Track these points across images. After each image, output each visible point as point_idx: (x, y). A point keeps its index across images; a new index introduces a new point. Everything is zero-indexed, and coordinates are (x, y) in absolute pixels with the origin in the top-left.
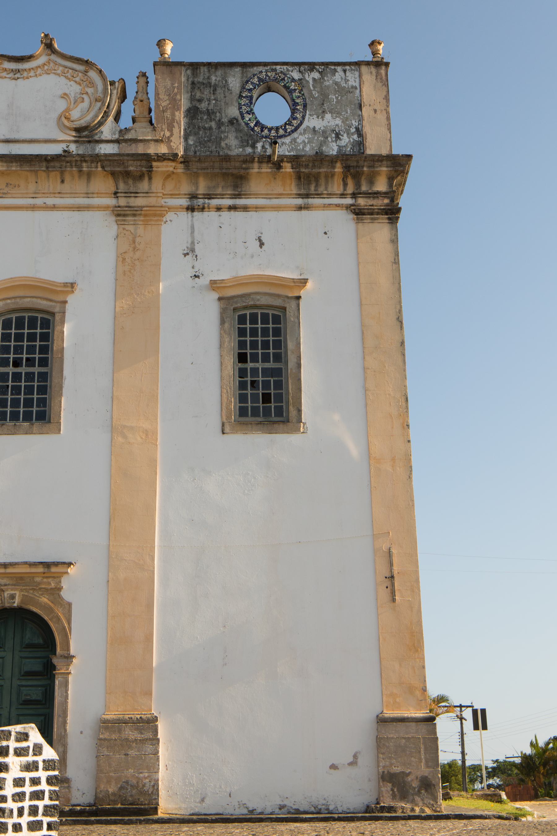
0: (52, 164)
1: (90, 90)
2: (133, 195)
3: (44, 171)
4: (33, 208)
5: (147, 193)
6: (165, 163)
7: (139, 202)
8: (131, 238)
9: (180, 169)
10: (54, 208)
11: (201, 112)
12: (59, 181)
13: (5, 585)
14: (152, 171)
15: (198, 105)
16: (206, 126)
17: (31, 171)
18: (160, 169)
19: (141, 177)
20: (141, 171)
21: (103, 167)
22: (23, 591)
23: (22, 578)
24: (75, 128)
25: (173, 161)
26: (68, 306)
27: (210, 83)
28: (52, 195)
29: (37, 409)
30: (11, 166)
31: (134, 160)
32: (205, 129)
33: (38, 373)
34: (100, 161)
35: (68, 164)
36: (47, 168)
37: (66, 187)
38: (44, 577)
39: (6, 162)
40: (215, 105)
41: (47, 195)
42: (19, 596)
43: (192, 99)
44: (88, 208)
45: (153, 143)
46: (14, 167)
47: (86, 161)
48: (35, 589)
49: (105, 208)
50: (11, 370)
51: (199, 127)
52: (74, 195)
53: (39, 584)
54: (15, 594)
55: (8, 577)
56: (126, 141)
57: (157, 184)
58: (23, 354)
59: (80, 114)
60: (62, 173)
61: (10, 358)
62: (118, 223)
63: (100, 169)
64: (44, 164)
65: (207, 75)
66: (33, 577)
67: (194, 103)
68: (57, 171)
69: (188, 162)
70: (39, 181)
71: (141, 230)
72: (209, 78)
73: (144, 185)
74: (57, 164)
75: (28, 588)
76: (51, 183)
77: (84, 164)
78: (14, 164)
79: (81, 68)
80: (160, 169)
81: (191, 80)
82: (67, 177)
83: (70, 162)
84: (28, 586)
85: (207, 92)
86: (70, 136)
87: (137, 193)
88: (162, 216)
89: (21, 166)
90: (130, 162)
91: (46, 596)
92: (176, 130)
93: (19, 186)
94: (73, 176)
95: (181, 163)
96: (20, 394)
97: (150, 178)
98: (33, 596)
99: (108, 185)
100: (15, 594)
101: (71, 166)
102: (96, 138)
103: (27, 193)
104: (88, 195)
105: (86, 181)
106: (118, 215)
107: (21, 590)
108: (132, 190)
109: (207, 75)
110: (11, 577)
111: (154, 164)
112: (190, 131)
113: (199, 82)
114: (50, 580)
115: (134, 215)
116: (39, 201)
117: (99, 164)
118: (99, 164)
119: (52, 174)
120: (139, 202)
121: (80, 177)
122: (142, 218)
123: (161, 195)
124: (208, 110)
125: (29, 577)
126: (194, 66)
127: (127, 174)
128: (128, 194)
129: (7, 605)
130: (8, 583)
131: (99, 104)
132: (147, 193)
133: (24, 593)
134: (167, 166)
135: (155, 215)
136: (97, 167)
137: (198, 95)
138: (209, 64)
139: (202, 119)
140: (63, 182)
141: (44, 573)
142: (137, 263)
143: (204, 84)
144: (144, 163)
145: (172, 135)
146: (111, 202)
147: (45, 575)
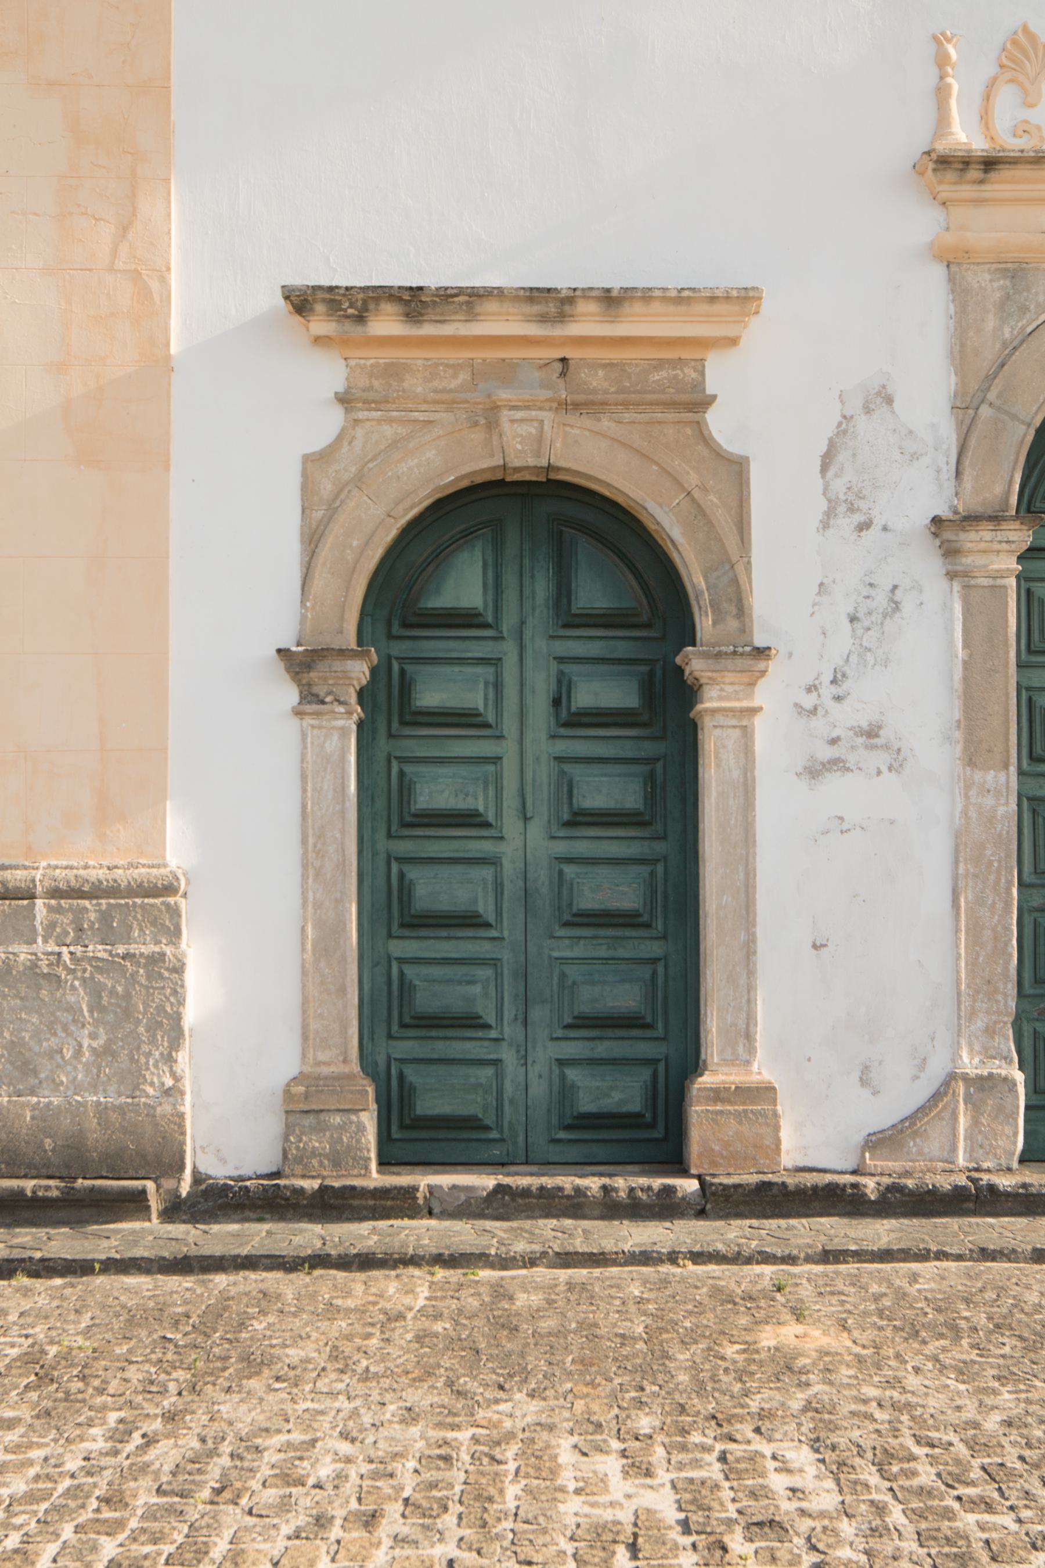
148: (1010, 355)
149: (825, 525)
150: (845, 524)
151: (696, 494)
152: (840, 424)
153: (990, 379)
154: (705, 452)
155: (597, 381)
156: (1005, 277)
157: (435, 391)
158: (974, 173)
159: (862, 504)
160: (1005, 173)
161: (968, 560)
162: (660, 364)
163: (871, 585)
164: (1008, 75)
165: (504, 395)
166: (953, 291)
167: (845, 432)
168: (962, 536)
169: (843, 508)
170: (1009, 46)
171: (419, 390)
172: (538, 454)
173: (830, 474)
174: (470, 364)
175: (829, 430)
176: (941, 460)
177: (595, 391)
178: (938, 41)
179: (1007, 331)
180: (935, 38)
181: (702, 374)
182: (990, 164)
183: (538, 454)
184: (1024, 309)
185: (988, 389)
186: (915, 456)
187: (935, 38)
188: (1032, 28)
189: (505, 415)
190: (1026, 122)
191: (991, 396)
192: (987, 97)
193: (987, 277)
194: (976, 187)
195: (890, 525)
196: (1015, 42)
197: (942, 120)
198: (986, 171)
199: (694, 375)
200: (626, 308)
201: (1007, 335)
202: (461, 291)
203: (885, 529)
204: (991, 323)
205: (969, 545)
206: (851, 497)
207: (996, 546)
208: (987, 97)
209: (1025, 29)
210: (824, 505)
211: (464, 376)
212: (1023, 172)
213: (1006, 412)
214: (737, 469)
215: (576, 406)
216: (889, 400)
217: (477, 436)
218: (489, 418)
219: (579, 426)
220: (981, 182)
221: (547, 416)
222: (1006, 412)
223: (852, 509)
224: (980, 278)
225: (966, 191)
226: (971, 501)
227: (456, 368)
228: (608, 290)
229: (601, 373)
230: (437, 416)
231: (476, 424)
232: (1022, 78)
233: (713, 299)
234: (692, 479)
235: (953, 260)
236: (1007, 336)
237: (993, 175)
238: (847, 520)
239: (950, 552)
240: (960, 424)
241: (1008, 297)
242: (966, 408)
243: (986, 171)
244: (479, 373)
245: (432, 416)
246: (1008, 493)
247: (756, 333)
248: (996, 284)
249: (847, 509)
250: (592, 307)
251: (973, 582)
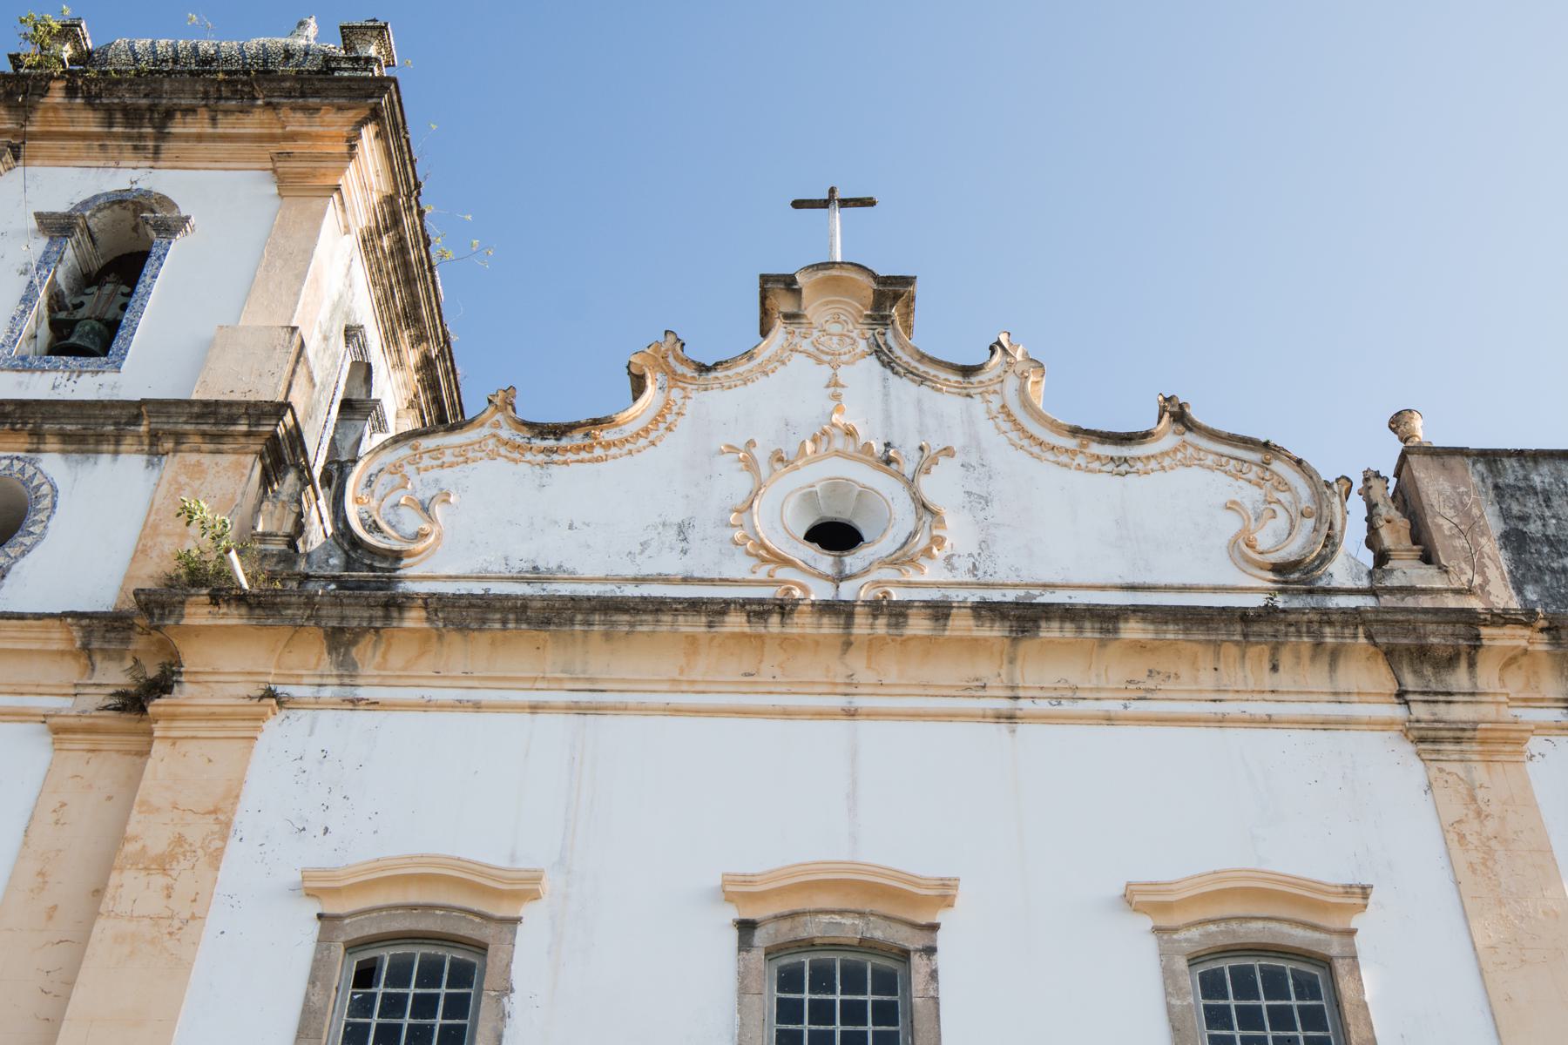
0: (1255, 628)
1: (1284, 497)
2: (1441, 698)
3: (1237, 643)
4: (1221, 721)
5: (1473, 694)
6: (1508, 630)
7: (1459, 712)
8: (1463, 789)
9: (1541, 644)
10: (1269, 721)
11: (1534, 540)
12: (1267, 666)
14: (1481, 646)
15: (1521, 526)
16: (1555, 565)
17: (1209, 641)
18: (1497, 643)
19: (1451, 662)
20: (1456, 648)
21: (1369, 636)
24: (1274, 564)
25: (1526, 625)
26: (1357, 939)
27: (1534, 489)
28: (1257, 696)
30: (1165, 632)
31: (1438, 623)
32: (1553, 571)
34: (1363, 623)
35: (1292, 629)
36: (1245, 635)
37: (1284, 680)
39: (1153, 622)
40: (1558, 526)
41: (1245, 696)
43: (1505, 515)
44: (1346, 723)
45: (1450, 595)
46: (1172, 633)
47: (1330, 623)
49: (1387, 725)
51: (1539, 568)
52: (1306, 695)
56: (1391, 591)
57: (1488, 675)
59: (1283, 538)
60: (1275, 649)
62: (1425, 756)
63: (1362, 640)
64: (1238, 628)
65: (1521, 473)
67: (1513, 523)
68: (1266, 643)
69: (1557, 629)
70: (1221, 666)
71: (1480, 773)
72: (1526, 478)
73: (1459, 679)
74: (1268, 629)
76: (1245, 670)
77: (1327, 630)
78: (1171, 627)
79: (1256, 457)
80: (1497, 643)
81: (1489, 481)
82: (1286, 658)
83: (1296, 624)
85: (1531, 502)
86: (1266, 580)
87: (1450, 694)
88: (1520, 742)
89: (1186, 631)
90: (1431, 627)
92: (1492, 573)
93: (1177, 676)
94: (1298, 658)
95: (1542, 630)
97: (1472, 665)
99: (1379, 678)
101: (1299, 634)
102: (1322, 584)
103: (1200, 691)
104: (1337, 697)
105: (1327, 668)
106: (1422, 740)
108: (1434, 686)
109: (1521, 473)
111: (1484, 631)
112: (1523, 575)
113: (1508, 486)
115: (1458, 740)
116: (1230, 708)
117: (1361, 630)
118: (1361, 630)
119: (1253, 651)
120: (1459, 712)
121: (1313, 658)
122: (1476, 747)
123: (1504, 699)
124: (1547, 537)
126: (1490, 458)
127: (1421, 654)
128: (1431, 696)
131: (1310, 523)
132: (1473, 694)
134: (1513, 637)
135: (1506, 741)
136: (1355, 636)
137: (1515, 508)
138: (1520, 454)
139: (1539, 552)
140: (1275, 668)
142: (1493, 843)
143: (1520, 489)
144: (1461, 629)
145: (1486, 581)
146: (1399, 712)
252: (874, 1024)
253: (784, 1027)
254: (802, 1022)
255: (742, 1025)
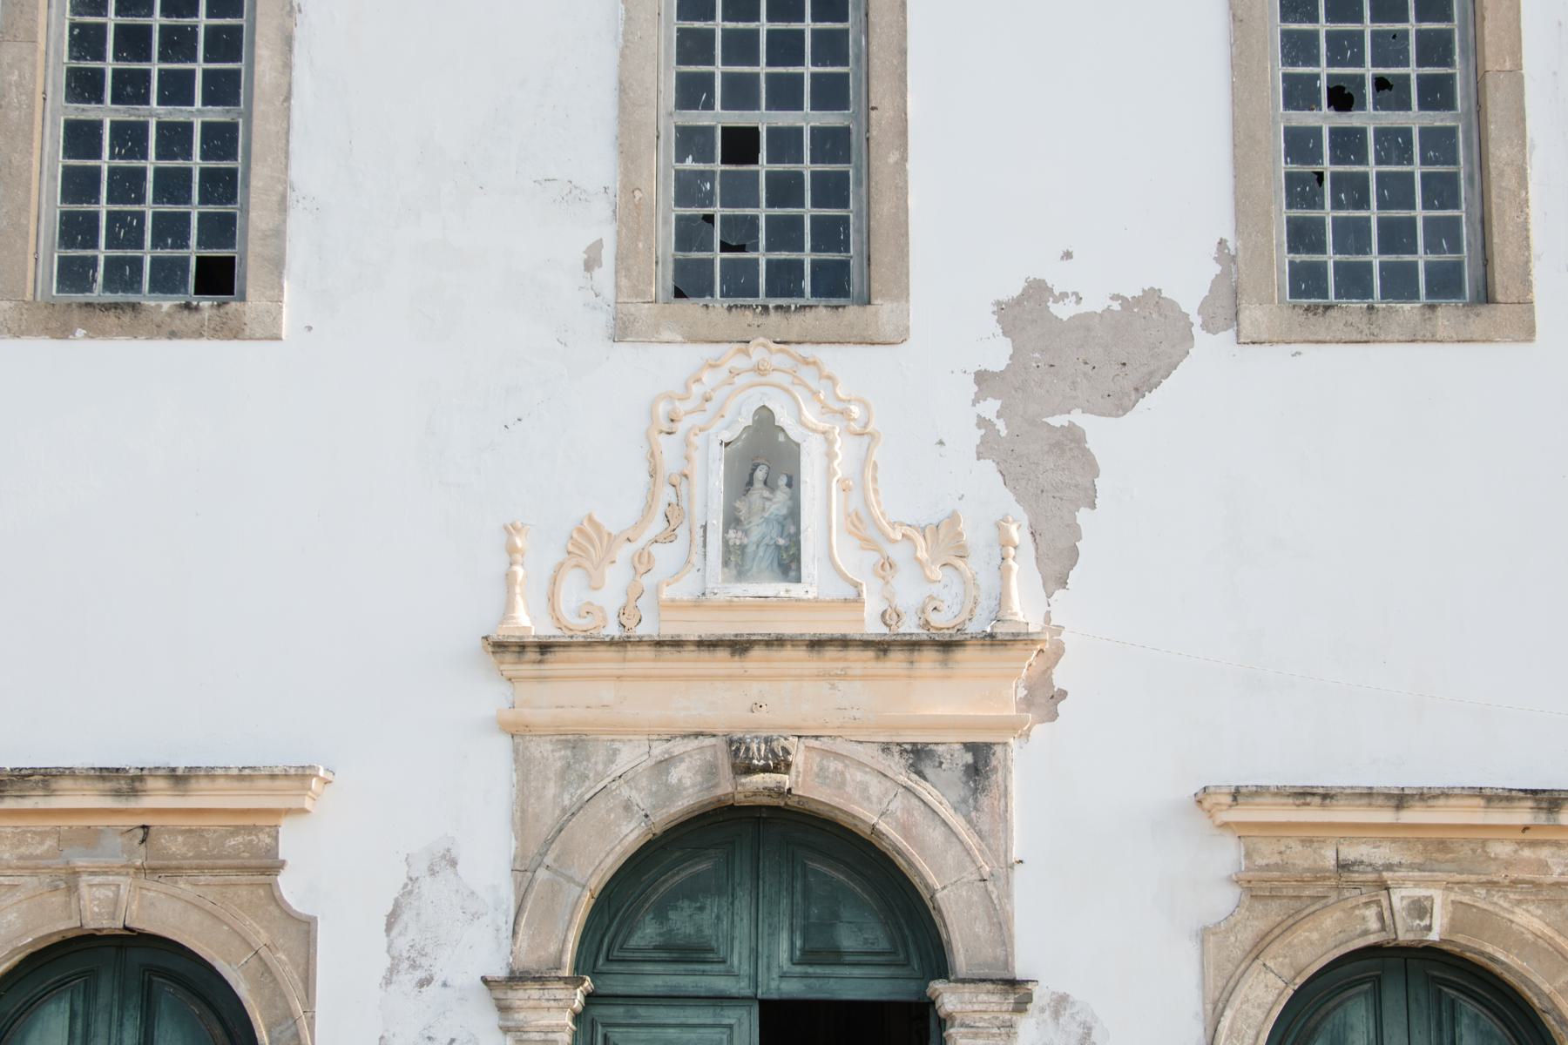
13: (1389, 867)
22: (1451, 889)
23: (1443, 845)
29: (1432, 258)
33: (1423, 131)
38: (1521, 844)
42: (1443, 906)
48: (1494, 883)
50: (1325, 118)
53: (1508, 864)
54: (1431, 899)
55: (1394, 840)
58: (1361, 64)
61: (1317, 77)
66: (1484, 842)
75: (1473, 878)
84: (1471, 872)
91: (1532, 908)
96: (1363, 203)
98: (1491, 908)
100: (1431, 899)
107: (1449, 886)
110: (1406, 840)
114: (1544, 853)
125: (1468, 841)
129: (1405, 937)
130: (1395, 860)
133: (1459, 898)
141: (1526, 828)
147: (1528, 836)
148: (569, 820)
149: (388, 981)
150: (407, 980)
151: (263, 953)
152: (406, 885)
153: (549, 843)
154: (277, 912)
155: (176, 846)
156: (566, 748)
157: (21, 858)
158: (532, 655)
159: (424, 961)
160: (560, 654)
161: (520, 1016)
162: (237, 830)
163: (429, 1038)
164: (574, 561)
165: (80, 862)
166: (516, 761)
167: (410, 893)
168: (511, 994)
169: (406, 965)
170: (575, 535)
171: (6, 856)
172: (113, 917)
173: (394, 933)
174: (57, 831)
175: (395, 892)
176: (501, 920)
177: (173, 856)
178: (511, 530)
179: (566, 797)
180: (506, 528)
181: (276, 839)
182: (545, 647)
183: (113, 917)
184: (584, 778)
185: (545, 853)
186: (476, 916)
187: (506, 528)
188: (596, 518)
189: (84, 880)
190: (591, 604)
191: (548, 860)
192: (554, 582)
193: (549, 747)
194: (536, 666)
195: (449, 982)
196: (581, 531)
197: (509, 606)
198: (542, 653)
199: (268, 840)
200: (193, 784)
201: (567, 802)
202: (35, 771)
203: (445, 985)
204: (551, 790)
205: (518, 1003)
206: (414, 954)
207: (546, 1004)
208: (554, 582)
209: (590, 519)
210: (387, 962)
211: (50, 843)
212: (574, 653)
213: (563, 875)
214: (306, 928)
215: (154, 870)
216: (453, 863)
217: (58, 899)
218: (70, 881)
219: (155, 890)
220: (540, 662)
221: (125, 882)
222: (563, 875)
223: (414, 966)
224: (542, 749)
225: (527, 669)
226: (528, 960)
227: (43, 835)
228: (174, 770)
229: (180, 839)
230: (22, 880)
231: (56, 888)
232: (587, 564)
233: (273, 777)
234: (262, 937)
235: (517, 732)
236: (567, 802)
237: (548, 656)
238: (409, 976)
239: (504, 1008)
240: (518, 885)
241: (569, 766)
242: (524, 871)
243: (542, 653)
244: (63, 840)
245: (16, 880)
246: (562, 952)
247: (322, 802)
248: (557, 755)
249: (410, 967)
250: (162, 784)
251: (525, 1037)
252: (814, 19)
253: (687, 25)
254: (713, 18)
255: (629, 19)
